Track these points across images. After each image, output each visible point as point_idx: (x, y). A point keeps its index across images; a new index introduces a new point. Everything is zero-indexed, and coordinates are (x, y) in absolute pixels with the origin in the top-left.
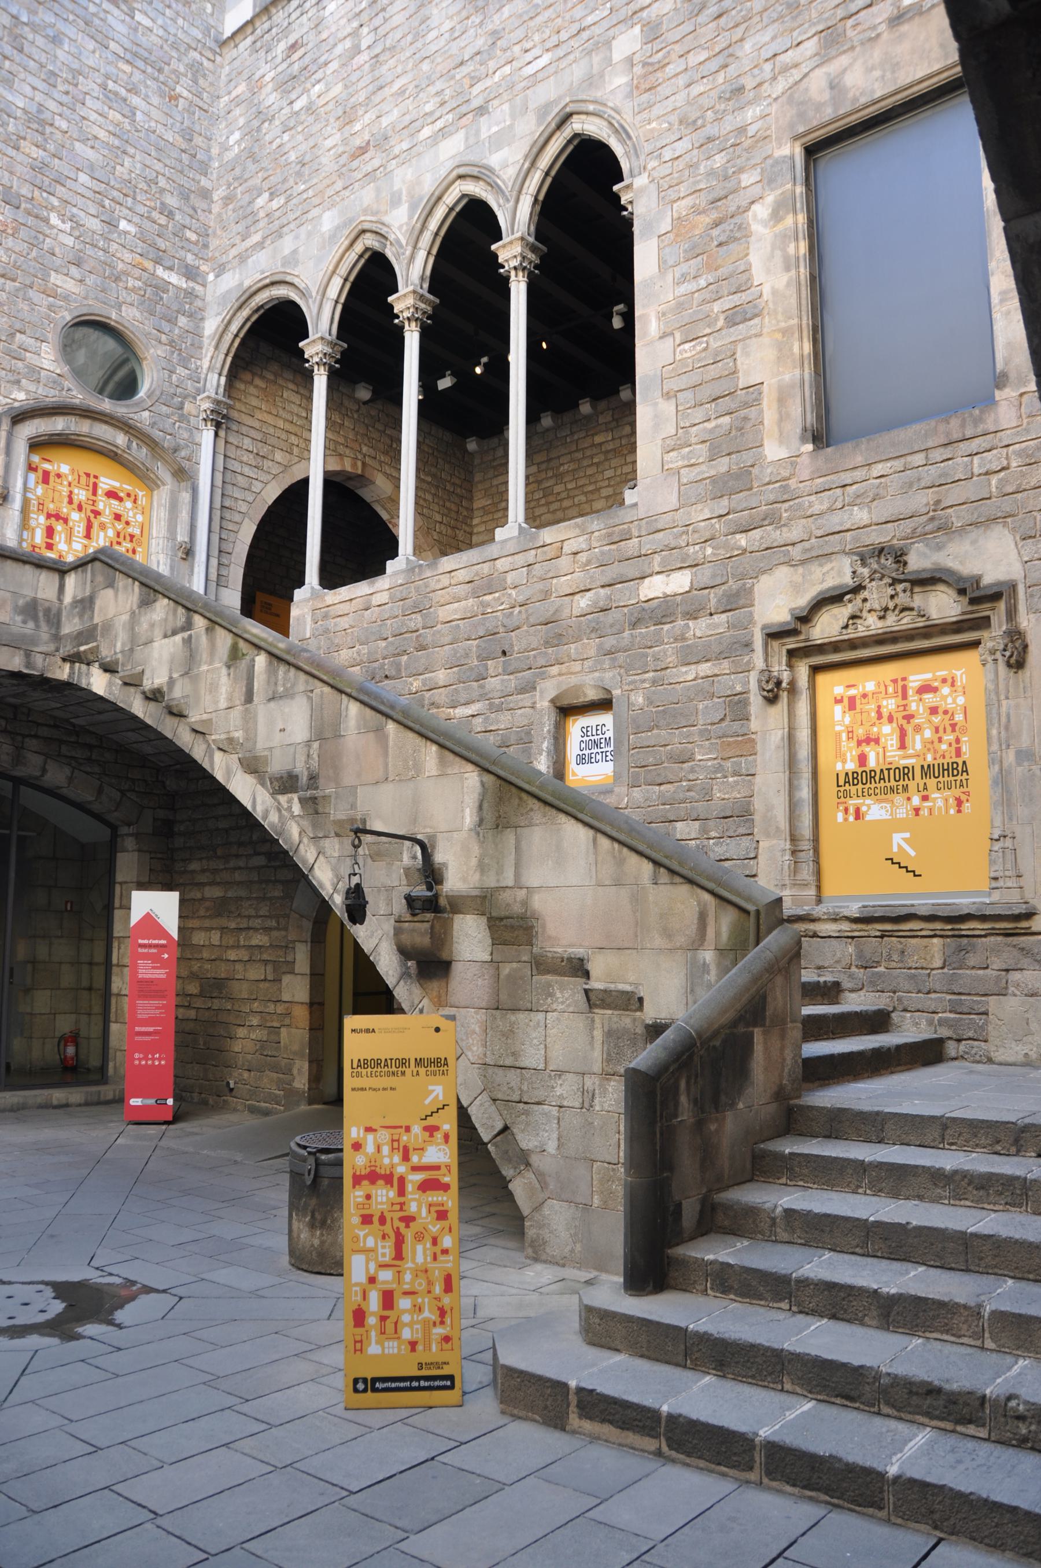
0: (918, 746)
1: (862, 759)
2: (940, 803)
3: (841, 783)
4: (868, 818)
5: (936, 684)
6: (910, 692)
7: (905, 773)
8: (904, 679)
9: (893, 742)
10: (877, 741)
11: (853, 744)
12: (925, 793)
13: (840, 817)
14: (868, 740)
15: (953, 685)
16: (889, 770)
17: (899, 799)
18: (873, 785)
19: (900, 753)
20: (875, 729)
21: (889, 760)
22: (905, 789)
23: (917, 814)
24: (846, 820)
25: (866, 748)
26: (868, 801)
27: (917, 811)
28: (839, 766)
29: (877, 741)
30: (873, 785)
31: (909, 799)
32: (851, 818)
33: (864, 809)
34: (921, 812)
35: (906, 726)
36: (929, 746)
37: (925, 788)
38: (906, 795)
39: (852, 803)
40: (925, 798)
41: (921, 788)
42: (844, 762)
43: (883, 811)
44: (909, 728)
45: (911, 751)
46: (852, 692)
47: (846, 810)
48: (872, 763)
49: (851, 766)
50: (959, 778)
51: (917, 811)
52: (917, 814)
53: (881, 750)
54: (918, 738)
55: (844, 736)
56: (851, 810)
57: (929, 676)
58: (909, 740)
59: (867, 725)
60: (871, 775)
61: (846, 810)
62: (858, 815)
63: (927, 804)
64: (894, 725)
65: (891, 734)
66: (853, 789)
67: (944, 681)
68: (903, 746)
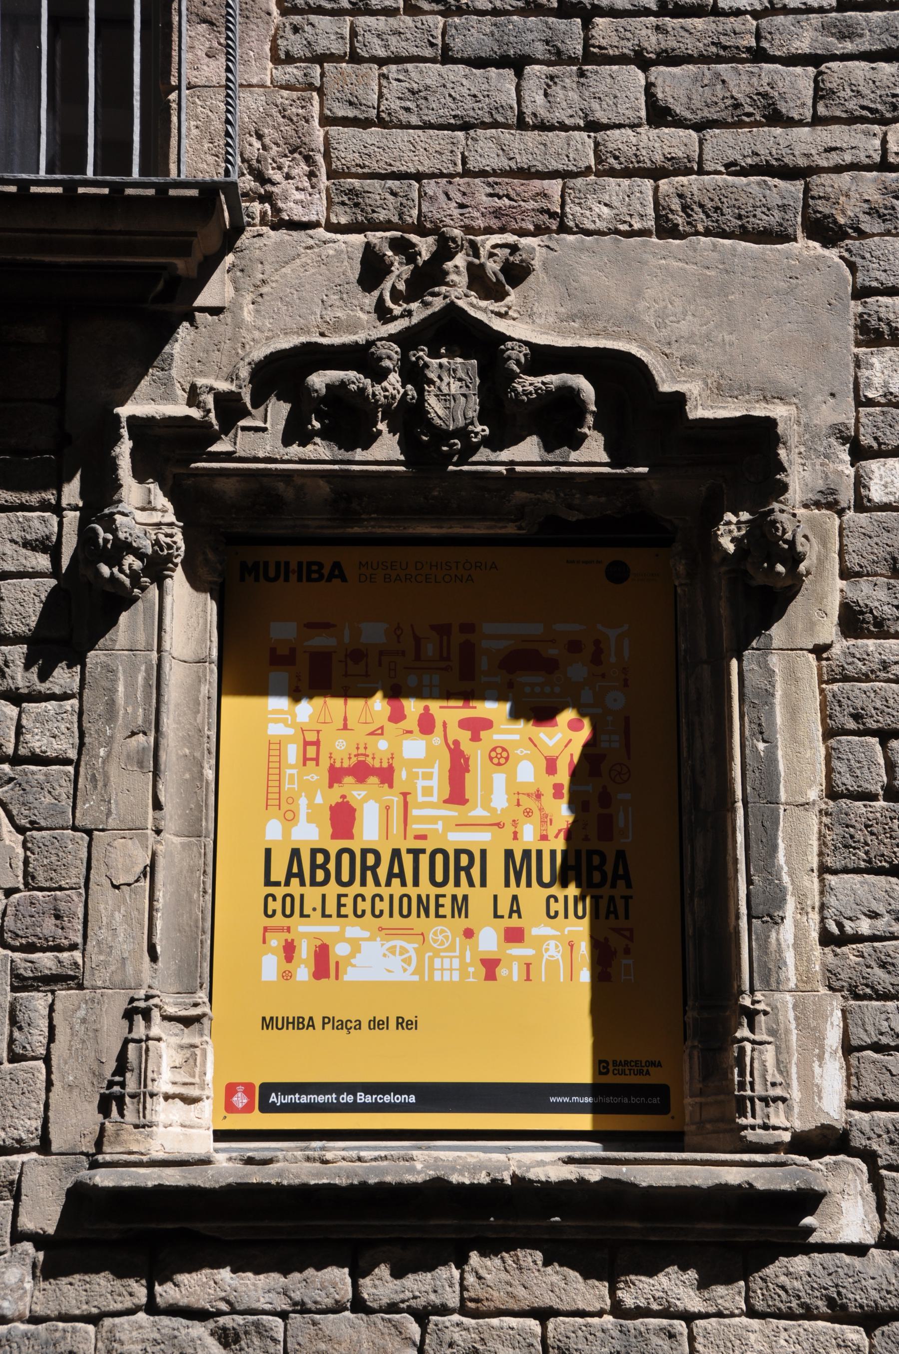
0: (500, 800)
1: (343, 818)
2: (554, 951)
3: (278, 874)
4: (350, 975)
5: (553, 652)
6: (484, 663)
7: (461, 865)
8: (468, 628)
9: (432, 782)
10: (386, 775)
11: (318, 775)
12: (515, 922)
13: (270, 965)
14: (361, 771)
15: (597, 658)
16: (416, 853)
17: (442, 931)
18: (370, 890)
19: (452, 812)
20: (383, 744)
21: (416, 827)
22: (461, 906)
23: (491, 975)
24: (287, 975)
25: (354, 792)
26: (354, 930)
27: (490, 966)
28: (273, 831)
29: (386, 775)
30: (370, 890)
31: (469, 933)
32: (303, 973)
33: (340, 950)
34: (501, 971)
35: (467, 746)
36: (527, 802)
37: (515, 909)
38: (462, 923)
39: (308, 931)
40: (514, 936)
41: (504, 908)
42: (290, 818)
43: (396, 962)
44: (477, 753)
45: (478, 813)
46: (321, 641)
47: (289, 950)
48: (369, 831)
49: (310, 832)
50: (606, 891)
51: (490, 966)
52: (491, 975)
53: (396, 801)
54: (499, 779)
55: (293, 753)
56: (305, 951)
57: (535, 629)
58: (473, 782)
59: (359, 733)
60: (365, 864)
61: (289, 950)
62: (323, 964)
63: (516, 950)
64: (437, 739)
65: (427, 762)
66: (313, 895)
67: (574, 646)
68: (457, 795)
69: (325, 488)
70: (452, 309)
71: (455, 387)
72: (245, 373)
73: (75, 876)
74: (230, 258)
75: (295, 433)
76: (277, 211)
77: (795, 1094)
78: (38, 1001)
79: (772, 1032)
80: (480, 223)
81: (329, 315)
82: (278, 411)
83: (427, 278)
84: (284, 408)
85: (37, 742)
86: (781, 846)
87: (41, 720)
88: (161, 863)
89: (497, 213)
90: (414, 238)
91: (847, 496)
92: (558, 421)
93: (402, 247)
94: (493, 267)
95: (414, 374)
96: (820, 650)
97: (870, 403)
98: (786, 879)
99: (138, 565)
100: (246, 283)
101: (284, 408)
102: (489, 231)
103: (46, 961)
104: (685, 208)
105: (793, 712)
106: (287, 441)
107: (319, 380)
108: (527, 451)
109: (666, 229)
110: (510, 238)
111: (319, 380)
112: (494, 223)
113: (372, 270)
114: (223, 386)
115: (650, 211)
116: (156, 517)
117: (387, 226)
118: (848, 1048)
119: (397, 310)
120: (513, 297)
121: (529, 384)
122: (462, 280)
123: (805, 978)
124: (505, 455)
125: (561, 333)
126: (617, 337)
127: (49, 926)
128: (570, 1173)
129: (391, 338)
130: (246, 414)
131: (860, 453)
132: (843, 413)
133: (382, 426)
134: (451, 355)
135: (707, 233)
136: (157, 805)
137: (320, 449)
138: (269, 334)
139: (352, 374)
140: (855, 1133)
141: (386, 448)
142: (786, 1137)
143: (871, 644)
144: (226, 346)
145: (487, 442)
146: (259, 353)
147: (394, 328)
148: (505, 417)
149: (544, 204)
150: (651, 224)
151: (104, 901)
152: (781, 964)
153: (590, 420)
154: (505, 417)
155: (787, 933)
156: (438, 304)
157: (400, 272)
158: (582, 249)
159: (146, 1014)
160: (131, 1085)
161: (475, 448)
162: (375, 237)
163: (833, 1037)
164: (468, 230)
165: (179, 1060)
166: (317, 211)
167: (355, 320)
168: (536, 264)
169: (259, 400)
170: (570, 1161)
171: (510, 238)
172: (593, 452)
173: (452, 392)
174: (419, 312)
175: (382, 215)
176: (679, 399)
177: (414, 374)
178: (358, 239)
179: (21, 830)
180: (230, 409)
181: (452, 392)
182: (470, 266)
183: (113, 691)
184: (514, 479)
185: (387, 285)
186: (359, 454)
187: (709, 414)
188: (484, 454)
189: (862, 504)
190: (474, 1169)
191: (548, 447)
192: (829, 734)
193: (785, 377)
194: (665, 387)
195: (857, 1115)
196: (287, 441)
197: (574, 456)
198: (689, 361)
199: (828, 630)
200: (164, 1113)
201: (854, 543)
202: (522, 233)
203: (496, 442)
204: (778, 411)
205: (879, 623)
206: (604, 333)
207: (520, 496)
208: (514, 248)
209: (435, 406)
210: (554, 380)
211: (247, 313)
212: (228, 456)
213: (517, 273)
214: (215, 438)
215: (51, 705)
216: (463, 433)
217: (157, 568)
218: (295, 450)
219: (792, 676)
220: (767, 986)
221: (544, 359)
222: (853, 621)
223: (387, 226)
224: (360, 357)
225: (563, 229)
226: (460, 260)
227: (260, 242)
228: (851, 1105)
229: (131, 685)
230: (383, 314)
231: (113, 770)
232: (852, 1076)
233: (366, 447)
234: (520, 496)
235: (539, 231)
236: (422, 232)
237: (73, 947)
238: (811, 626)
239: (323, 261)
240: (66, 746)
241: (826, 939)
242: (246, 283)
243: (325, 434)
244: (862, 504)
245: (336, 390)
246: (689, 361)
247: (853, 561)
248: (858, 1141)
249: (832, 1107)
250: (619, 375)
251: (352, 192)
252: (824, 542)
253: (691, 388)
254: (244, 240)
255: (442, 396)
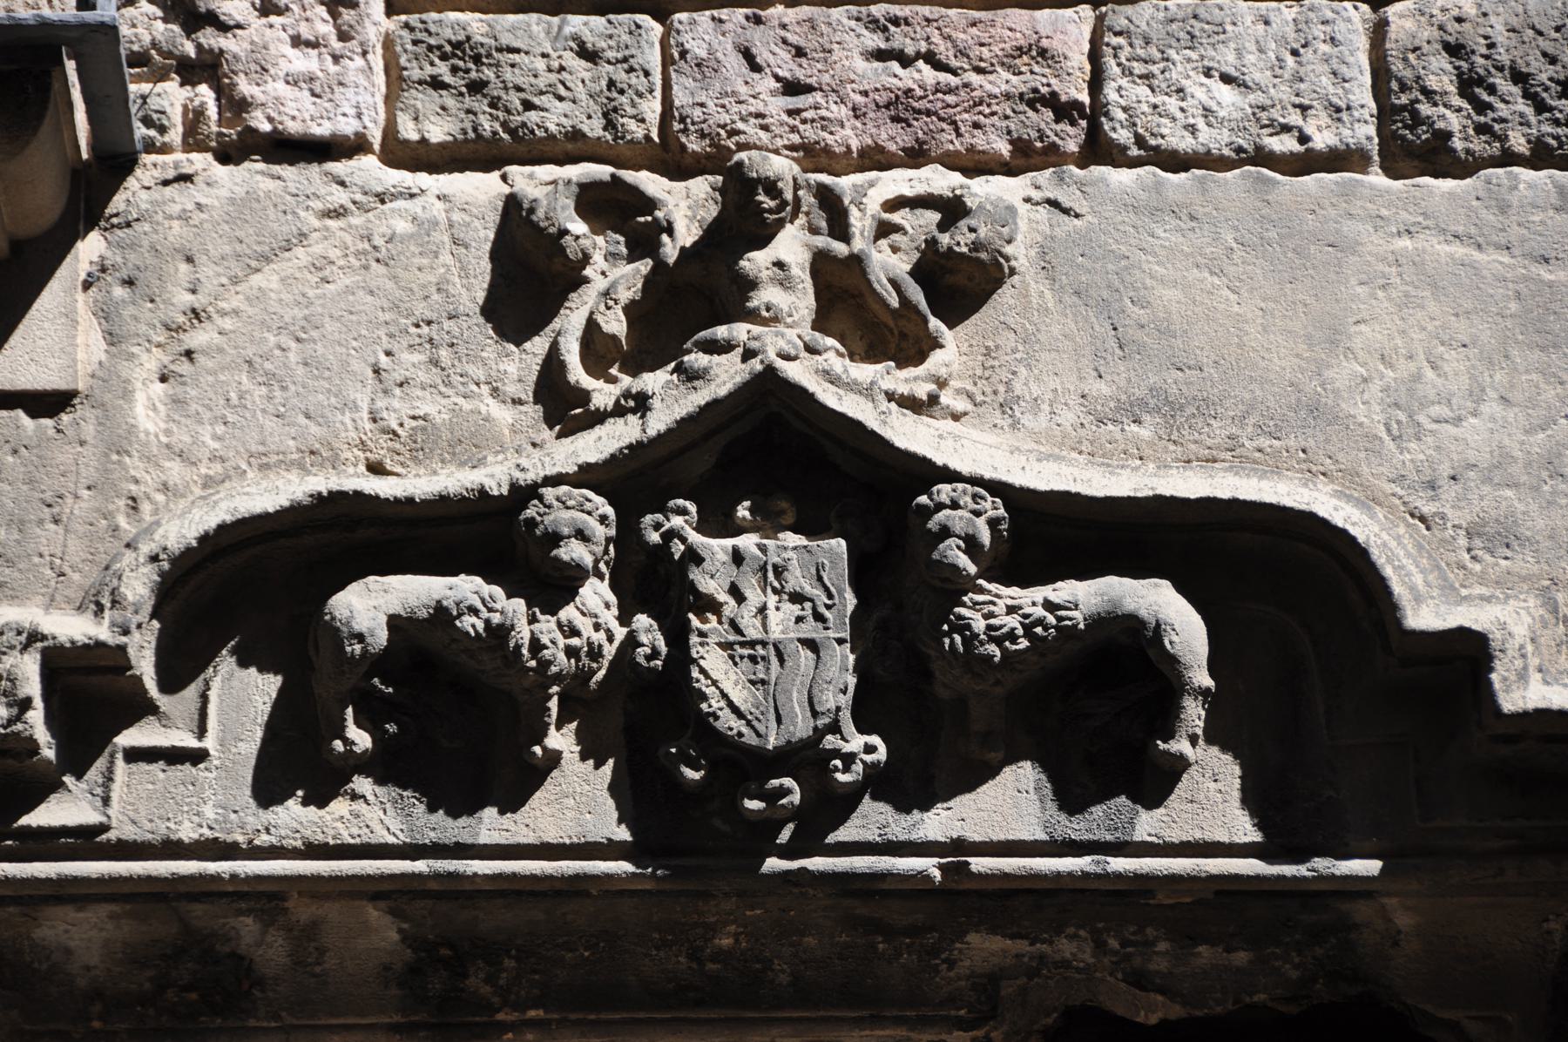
69: (383, 932)
70: (769, 392)
71: (782, 621)
72: (139, 586)
74: (90, 248)
75: (294, 762)
76: (235, 106)
80: (850, 137)
81: (396, 410)
82: (241, 697)
83: (692, 298)
84: (262, 688)
89: (899, 107)
90: (649, 182)
92: (1098, 720)
93: (613, 207)
94: (889, 265)
95: (654, 582)
100: (139, 317)
101: (262, 688)
102: (875, 159)
104: (1468, 84)
106: (268, 791)
107: (368, 606)
108: (1007, 808)
109: (1413, 150)
110: (939, 180)
111: (368, 606)
112: (893, 138)
113: (527, 278)
114: (72, 627)
115: (1362, 94)
117: (570, 148)
119: (603, 394)
120: (953, 350)
121: (1004, 609)
122: (800, 303)
124: (936, 823)
125: (1097, 454)
126: (1272, 466)
129: (587, 476)
130: (142, 708)
133: (561, 740)
134: (768, 523)
135: (1541, 156)
137: (372, 814)
139: (466, 587)
141: (575, 804)
144: (81, 507)
145: (881, 783)
146: (182, 528)
147: (595, 445)
148: (933, 714)
149: (1039, 78)
150: (1365, 132)
153: (1194, 713)
154: (933, 714)
156: (726, 374)
157: (611, 280)
158: (1158, 209)
161: (845, 804)
162: (534, 182)
164: (813, 156)
166: (358, 104)
167: (481, 429)
168: (1020, 253)
169: (182, 664)
171: (939, 180)
172: (1207, 808)
173: (775, 633)
174: (670, 401)
175: (553, 118)
176: (1468, 653)
177: (654, 582)
178: (481, 190)
180: (91, 697)
181: (775, 633)
182: (821, 263)
184: (965, 897)
185: (571, 323)
186: (490, 826)
188: (872, 819)
191: (1071, 799)
194: (1424, 616)
196: (268, 791)
197: (1148, 824)
198: (1494, 536)
202: (976, 165)
203: (908, 785)
206: (1233, 455)
207: (984, 947)
208: (952, 210)
209: (720, 676)
210: (1082, 596)
211: (147, 409)
212: (85, 841)
213: (960, 281)
214: (44, 786)
216: (807, 758)
218: (294, 817)
221: (1050, 534)
223: (570, 148)
224: (490, 534)
225: (1098, 150)
226: (792, 245)
227: (181, 200)
230: (560, 404)
233: (512, 802)
234: (984, 947)
235: (1027, 157)
236: (678, 167)
239: (375, 254)
242: (139, 317)
243: (387, 766)
245: (418, 636)
246: (1494, 536)
250: (1285, 583)
251: (461, 50)
253: (1505, 618)
254: (133, 194)
255: (740, 647)
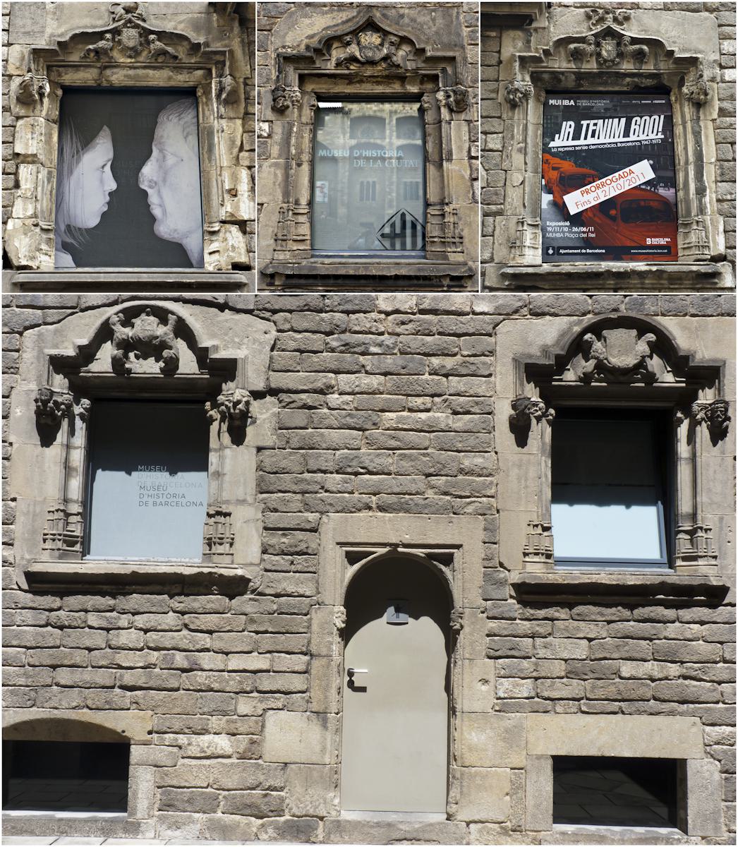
70: (609, 27)
73: (502, 184)
77: (711, 245)
78: (491, 219)
79: (704, 227)
85: (491, 146)
86: (705, 174)
87: (493, 139)
88: (527, 180)
91: (719, 79)
96: (714, 120)
97: (724, 54)
98: (707, 184)
99: (521, 95)
100: (551, 21)
103: (493, 208)
105: (707, 137)
111: (572, 46)
116: (526, 83)
118: (725, 232)
123: (713, 212)
127: (494, 198)
128: (647, 268)
131: (722, 67)
132: (717, 57)
136: (526, 163)
138: (557, 33)
140: (728, 256)
142: (709, 257)
143: (728, 119)
147: (593, 32)
151: (510, 191)
152: (706, 207)
155: (707, 199)
159: (523, 223)
160: (518, 244)
163: (721, 228)
165: (532, 236)
167: (583, 30)
168: (632, 17)
170: (648, 265)
173: (608, 48)
174: (599, 28)
178: (582, 10)
179: (486, 170)
183: (513, 131)
187: (678, 56)
189: (723, 81)
190: (619, 267)
192: (717, 143)
193: (701, 47)
195: (729, 251)
199: (715, 115)
200: (527, 251)
201: (721, 91)
204: (699, 56)
205: (729, 113)
209: (604, 53)
210: (638, 46)
213: (627, 19)
215: (495, 135)
217: (526, 95)
219: (706, 127)
220: (702, 214)
221: (634, 41)
222: (722, 112)
224: (582, 40)
225: (639, 8)
228: (727, 248)
229: (518, 129)
231: (513, 154)
232: (726, 239)
237: (501, 204)
238: (711, 114)
240: (499, 147)
241: (718, 201)
244: (723, 81)
246: (674, 42)
247: (721, 96)
248: (729, 258)
249: (721, 249)
250: (655, 44)
252: (713, 91)
255: (606, 51)
